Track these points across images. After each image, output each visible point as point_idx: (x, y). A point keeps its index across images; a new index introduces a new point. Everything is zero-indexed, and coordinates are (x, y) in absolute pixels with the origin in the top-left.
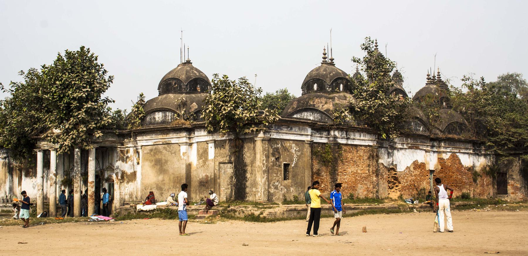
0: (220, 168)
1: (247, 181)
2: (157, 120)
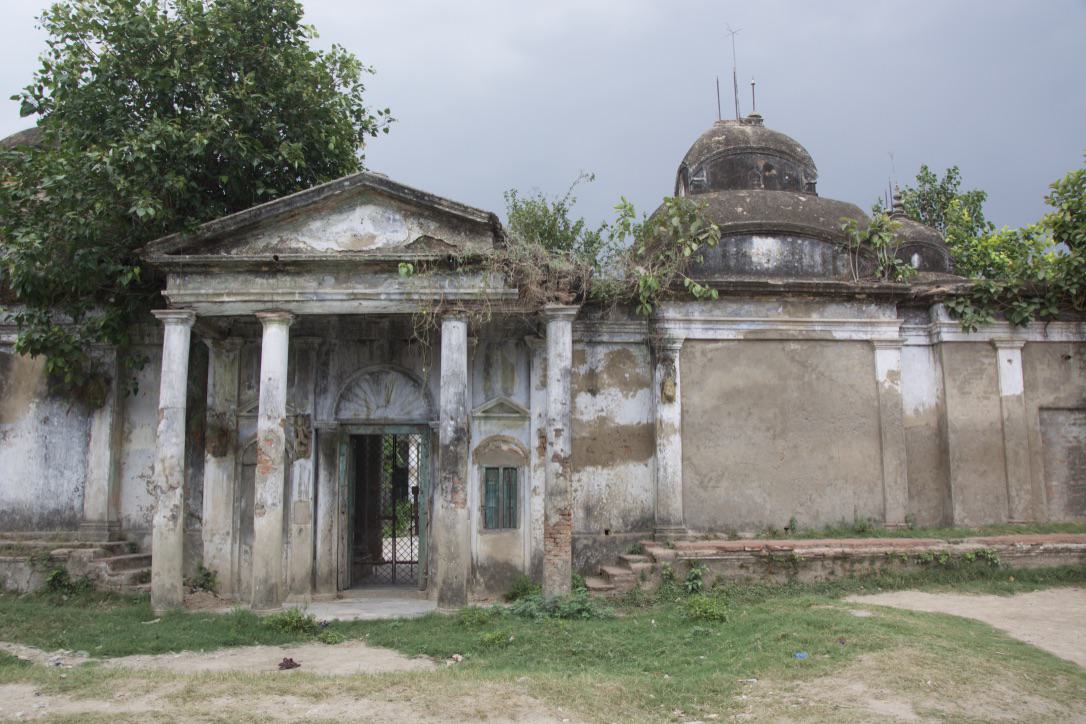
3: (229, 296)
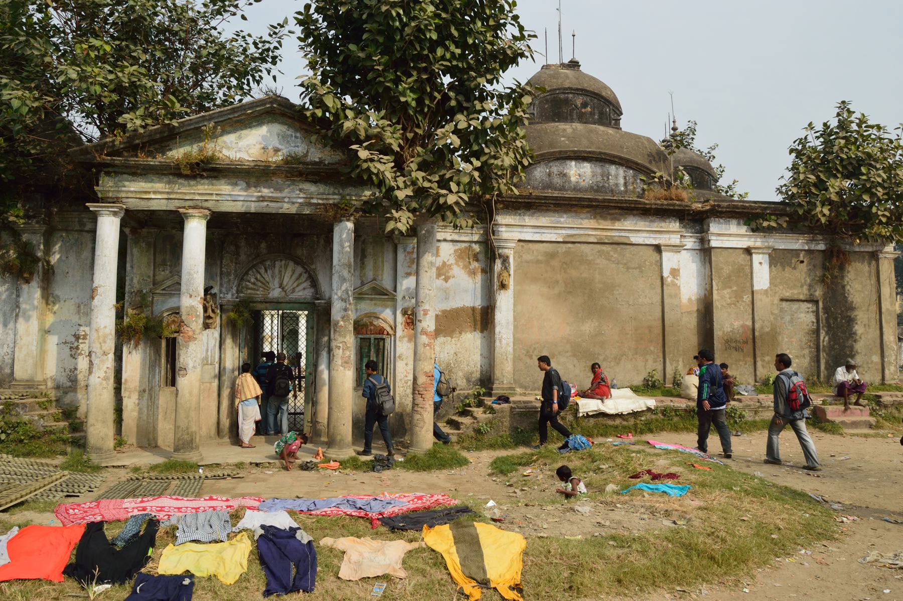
0: (782, 310)
1: (855, 341)
2: (573, 179)
3: (151, 194)
